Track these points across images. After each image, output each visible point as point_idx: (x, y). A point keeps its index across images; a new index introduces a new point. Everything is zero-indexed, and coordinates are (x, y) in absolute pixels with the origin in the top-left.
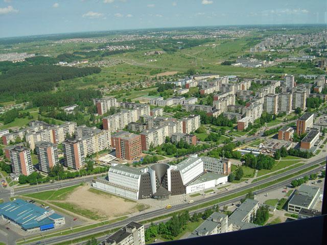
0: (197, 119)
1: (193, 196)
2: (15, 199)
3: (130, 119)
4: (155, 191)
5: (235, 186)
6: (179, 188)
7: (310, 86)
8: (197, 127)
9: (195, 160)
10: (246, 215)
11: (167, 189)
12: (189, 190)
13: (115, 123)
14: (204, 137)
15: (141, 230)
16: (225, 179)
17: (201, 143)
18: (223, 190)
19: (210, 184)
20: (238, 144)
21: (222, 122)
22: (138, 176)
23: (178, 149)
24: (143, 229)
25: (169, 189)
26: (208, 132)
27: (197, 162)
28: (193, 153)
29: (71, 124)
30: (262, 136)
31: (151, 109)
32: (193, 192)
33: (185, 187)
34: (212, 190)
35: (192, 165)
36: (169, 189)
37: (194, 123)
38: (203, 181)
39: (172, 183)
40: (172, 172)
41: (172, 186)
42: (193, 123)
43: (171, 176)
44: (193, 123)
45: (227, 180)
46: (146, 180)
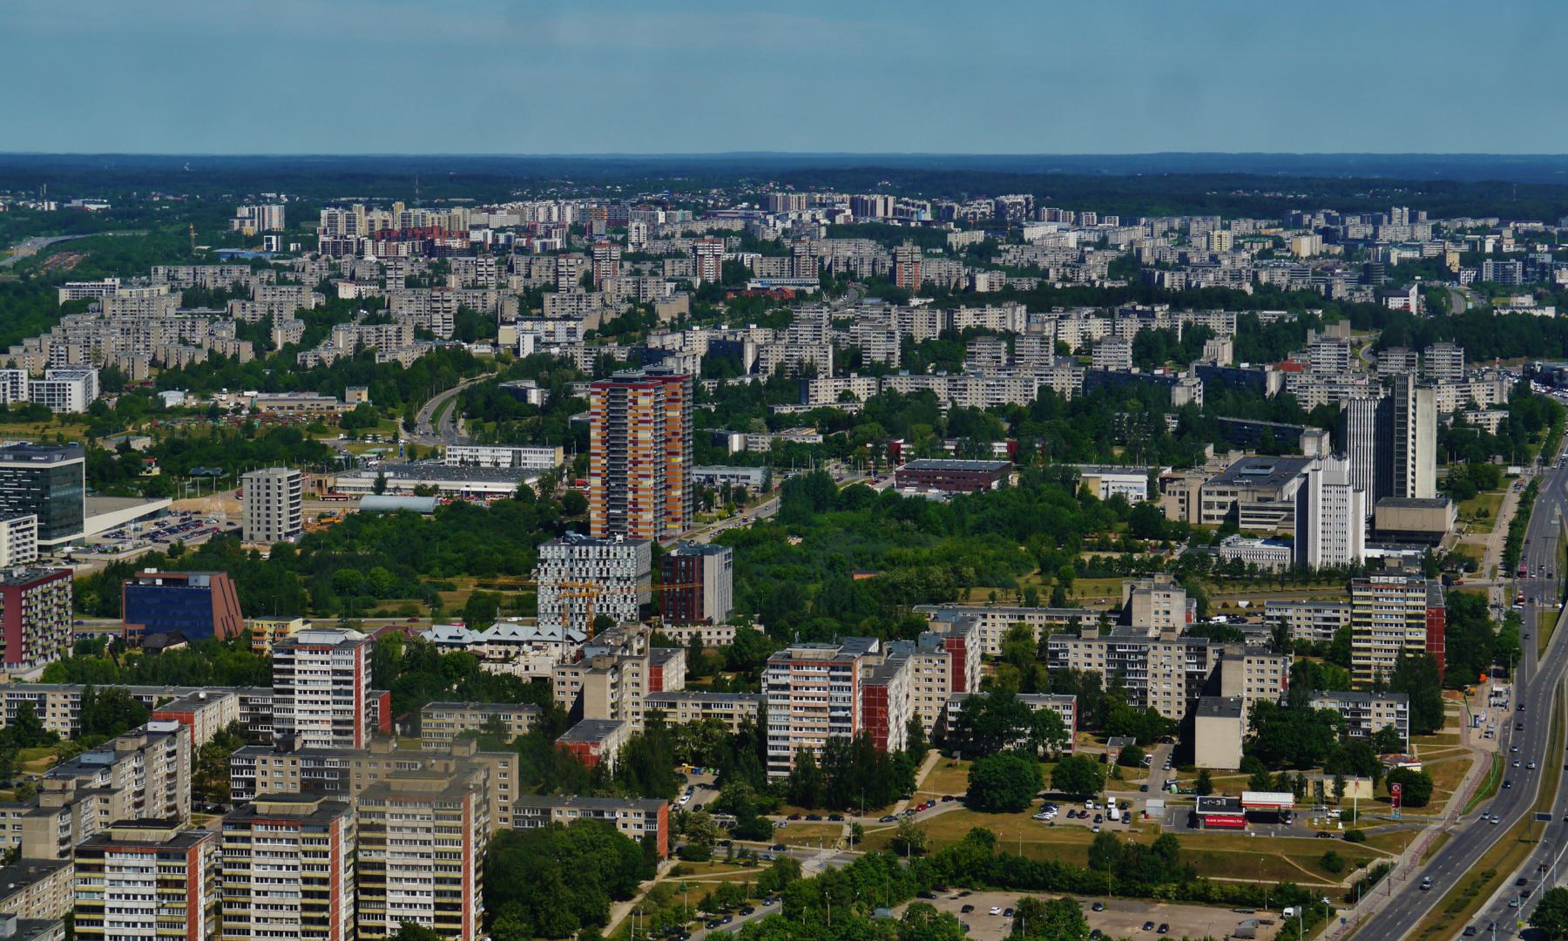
7: (519, 723)
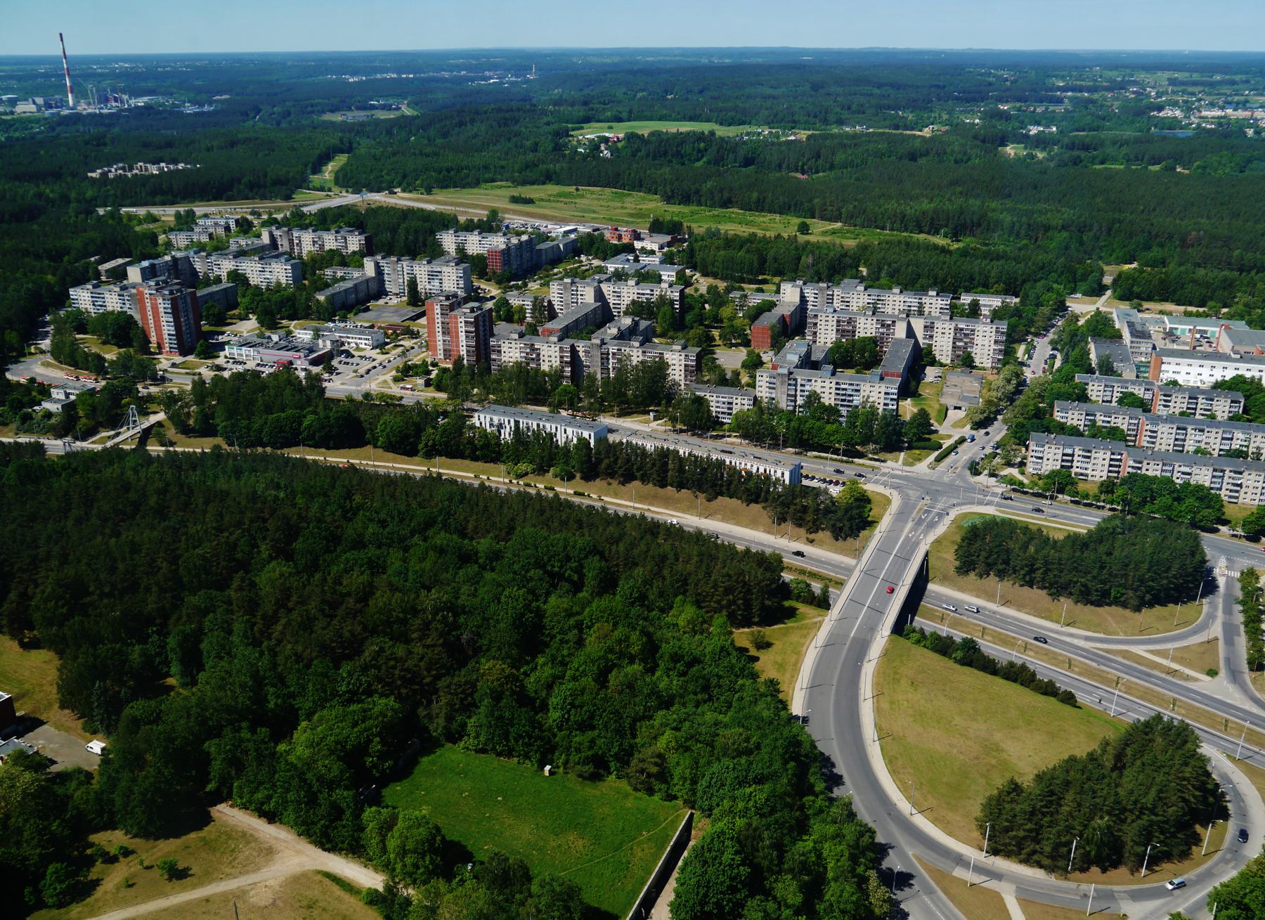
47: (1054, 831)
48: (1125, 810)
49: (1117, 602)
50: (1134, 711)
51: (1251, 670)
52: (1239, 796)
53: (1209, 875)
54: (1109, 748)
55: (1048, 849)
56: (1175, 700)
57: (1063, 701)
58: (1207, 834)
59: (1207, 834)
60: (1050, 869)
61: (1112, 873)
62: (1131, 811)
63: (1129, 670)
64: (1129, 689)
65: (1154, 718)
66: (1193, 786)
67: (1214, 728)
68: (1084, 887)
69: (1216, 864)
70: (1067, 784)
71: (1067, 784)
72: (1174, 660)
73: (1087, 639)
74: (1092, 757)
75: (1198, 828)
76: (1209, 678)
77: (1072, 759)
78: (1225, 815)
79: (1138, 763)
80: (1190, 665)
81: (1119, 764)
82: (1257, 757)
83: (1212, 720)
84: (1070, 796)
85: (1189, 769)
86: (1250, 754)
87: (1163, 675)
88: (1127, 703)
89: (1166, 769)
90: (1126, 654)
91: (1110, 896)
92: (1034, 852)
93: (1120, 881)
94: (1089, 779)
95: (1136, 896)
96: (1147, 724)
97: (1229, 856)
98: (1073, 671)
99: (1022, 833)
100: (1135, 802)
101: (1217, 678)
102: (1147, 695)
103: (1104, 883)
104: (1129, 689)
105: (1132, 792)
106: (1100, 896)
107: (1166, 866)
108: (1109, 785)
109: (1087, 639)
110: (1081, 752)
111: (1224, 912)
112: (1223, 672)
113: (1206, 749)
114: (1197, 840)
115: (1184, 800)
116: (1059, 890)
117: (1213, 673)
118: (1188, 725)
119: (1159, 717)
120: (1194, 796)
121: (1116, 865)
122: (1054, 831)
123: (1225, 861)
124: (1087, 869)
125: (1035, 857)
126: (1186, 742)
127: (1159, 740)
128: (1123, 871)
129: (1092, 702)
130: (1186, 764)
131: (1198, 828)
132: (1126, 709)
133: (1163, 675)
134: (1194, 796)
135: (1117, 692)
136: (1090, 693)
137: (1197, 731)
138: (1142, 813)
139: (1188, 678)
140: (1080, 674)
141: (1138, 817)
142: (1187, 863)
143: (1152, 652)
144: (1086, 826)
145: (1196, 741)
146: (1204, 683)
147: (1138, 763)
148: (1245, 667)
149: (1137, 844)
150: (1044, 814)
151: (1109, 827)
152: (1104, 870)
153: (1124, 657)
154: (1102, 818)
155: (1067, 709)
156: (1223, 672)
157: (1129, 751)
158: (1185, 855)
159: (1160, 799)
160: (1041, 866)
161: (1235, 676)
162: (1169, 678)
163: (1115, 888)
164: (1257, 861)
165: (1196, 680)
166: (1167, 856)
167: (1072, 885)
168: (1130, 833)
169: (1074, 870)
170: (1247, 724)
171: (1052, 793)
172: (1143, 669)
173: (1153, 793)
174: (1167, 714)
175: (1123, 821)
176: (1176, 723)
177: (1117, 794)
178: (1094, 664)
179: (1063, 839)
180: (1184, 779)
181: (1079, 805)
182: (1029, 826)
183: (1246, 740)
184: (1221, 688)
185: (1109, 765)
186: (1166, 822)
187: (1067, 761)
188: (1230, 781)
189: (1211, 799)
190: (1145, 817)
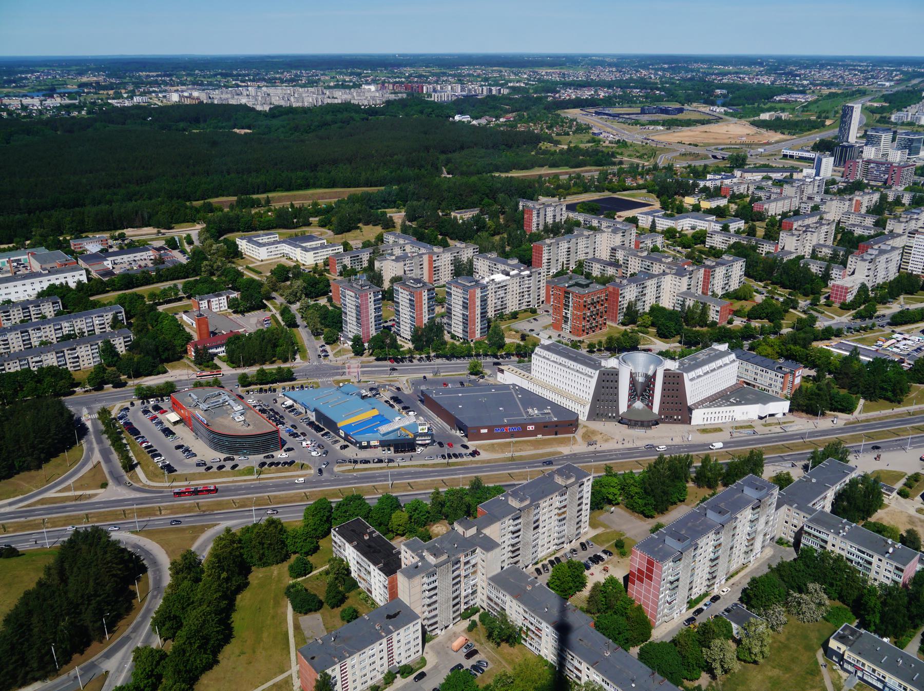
0: (738, 268)
1: (704, 431)
2: (450, 386)
3: (590, 250)
4: (623, 408)
5: (803, 424)
6: (677, 409)
8: (734, 285)
9: (722, 355)
10: (821, 493)
11: (651, 408)
12: (699, 417)
13: (556, 254)
14: (748, 306)
15: (586, 484)
16: (786, 405)
17: (738, 323)
18: (777, 429)
19: (750, 412)
20: (828, 334)
21: (798, 279)
22: (594, 371)
23: (687, 330)
24: (590, 483)
25: (656, 409)
26: (759, 298)
27: (726, 360)
28: (720, 341)
29: (466, 247)
30: (889, 324)
31: (639, 235)
32: (705, 422)
33: (690, 410)
34: (751, 427)
35: (713, 365)
36: (656, 409)
37: (731, 275)
38: (732, 404)
39: (663, 396)
40: (668, 374)
41: (662, 402)
42: (728, 277)
43: (664, 383)
44: (728, 277)
45: (787, 410)
46: (608, 381)
47: (34, 650)
48: (78, 605)
49: (22, 469)
50: (63, 536)
51: (127, 472)
52: (147, 553)
53: (148, 611)
54: (52, 571)
55: (35, 665)
56: (87, 515)
57: (8, 557)
58: (137, 588)
59: (137, 588)
60: (43, 678)
61: (89, 651)
62: (82, 604)
63: (49, 511)
64: (54, 523)
65: (73, 535)
66: (117, 564)
67: (118, 519)
68: (72, 673)
69: (150, 602)
70: (30, 613)
71: (30, 613)
72: (76, 489)
73: (10, 504)
74: (40, 584)
75: (131, 587)
76: (103, 490)
77: (27, 594)
78: (144, 569)
79: (75, 569)
80: (89, 487)
81: (64, 579)
82: (150, 523)
83: (115, 515)
84: (35, 620)
85: (109, 555)
86: (144, 524)
87: (74, 503)
88: (56, 534)
89: (95, 563)
90: (42, 502)
91: (93, 666)
92: (27, 673)
93: (95, 653)
94: (45, 600)
95: (108, 656)
96: (70, 541)
97: (155, 593)
98: (8, 532)
99: (11, 667)
100: (82, 597)
101: (109, 487)
102: (67, 521)
103: (85, 661)
104: (54, 523)
105: (77, 590)
106: (85, 671)
107: (121, 623)
108: (60, 595)
109: (10, 504)
110: (32, 586)
111: (164, 628)
112: (111, 482)
113: (115, 535)
114: (133, 595)
115: (114, 576)
116: (56, 686)
117: (104, 485)
118: (97, 527)
119: (77, 532)
120: (120, 570)
121: (88, 644)
122: (34, 650)
123: (154, 597)
124: (70, 659)
125: (29, 676)
126: (100, 538)
127: (83, 547)
128: (95, 645)
129: (31, 546)
130: (106, 553)
131: (131, 587)
132: (50, 538)
133: (74, 503)
134: (120, 570)
135: (44, 530)
136: (27, 541)
137: (105, 528)
138: (89, 601)
139: (90, 496)
140: (15, 531)
141: (89, 604)
142: (132, 613)
143: (60, 491)
144: (55, 633)
145: (107, 534)
146: (102, 495)
147: (75, 569)
148: (123, 472)
149: (95, 622)
150: (22, 644)
151: (71, 623)
152: (82, 653)
153: (42, 504)
154: (64, 620)
155: (14, 561)
156: (111, 482)
157: (66, 566)
158: (129, 609)
159: (98, 584)
160: (35, 680)
161: (119, 480)
162: (78, 502)
163: (93, 659)
164: (170, 586)
165: (95, 495)
166: (119, 617)
167: (64, 677)
168: (87, 617)
169: (61, 666)
170: (135, 506)
171: (21, 626)
172: (58, 505)
173: (91, 583)
174: (82, 527)
175: (80, 613)
176: (89, 530)
177: (67, 598)
178: (23, 519)
179: (43, 651)
180: (108, 563)
181: (44, 621)
182: (14, 658)
183: (139, 516)
184: (114, 492)
185: (56, 582)
186: (108, 596)
187: (24, 597)
188: (139, 547)
189: (131, 565)
190: (93, 602)
